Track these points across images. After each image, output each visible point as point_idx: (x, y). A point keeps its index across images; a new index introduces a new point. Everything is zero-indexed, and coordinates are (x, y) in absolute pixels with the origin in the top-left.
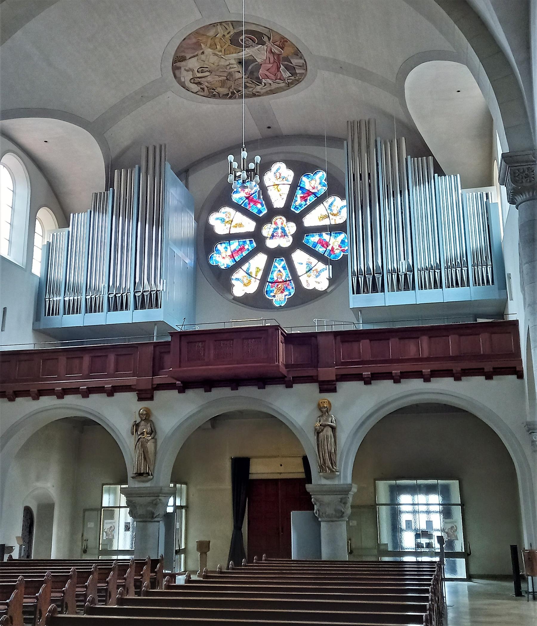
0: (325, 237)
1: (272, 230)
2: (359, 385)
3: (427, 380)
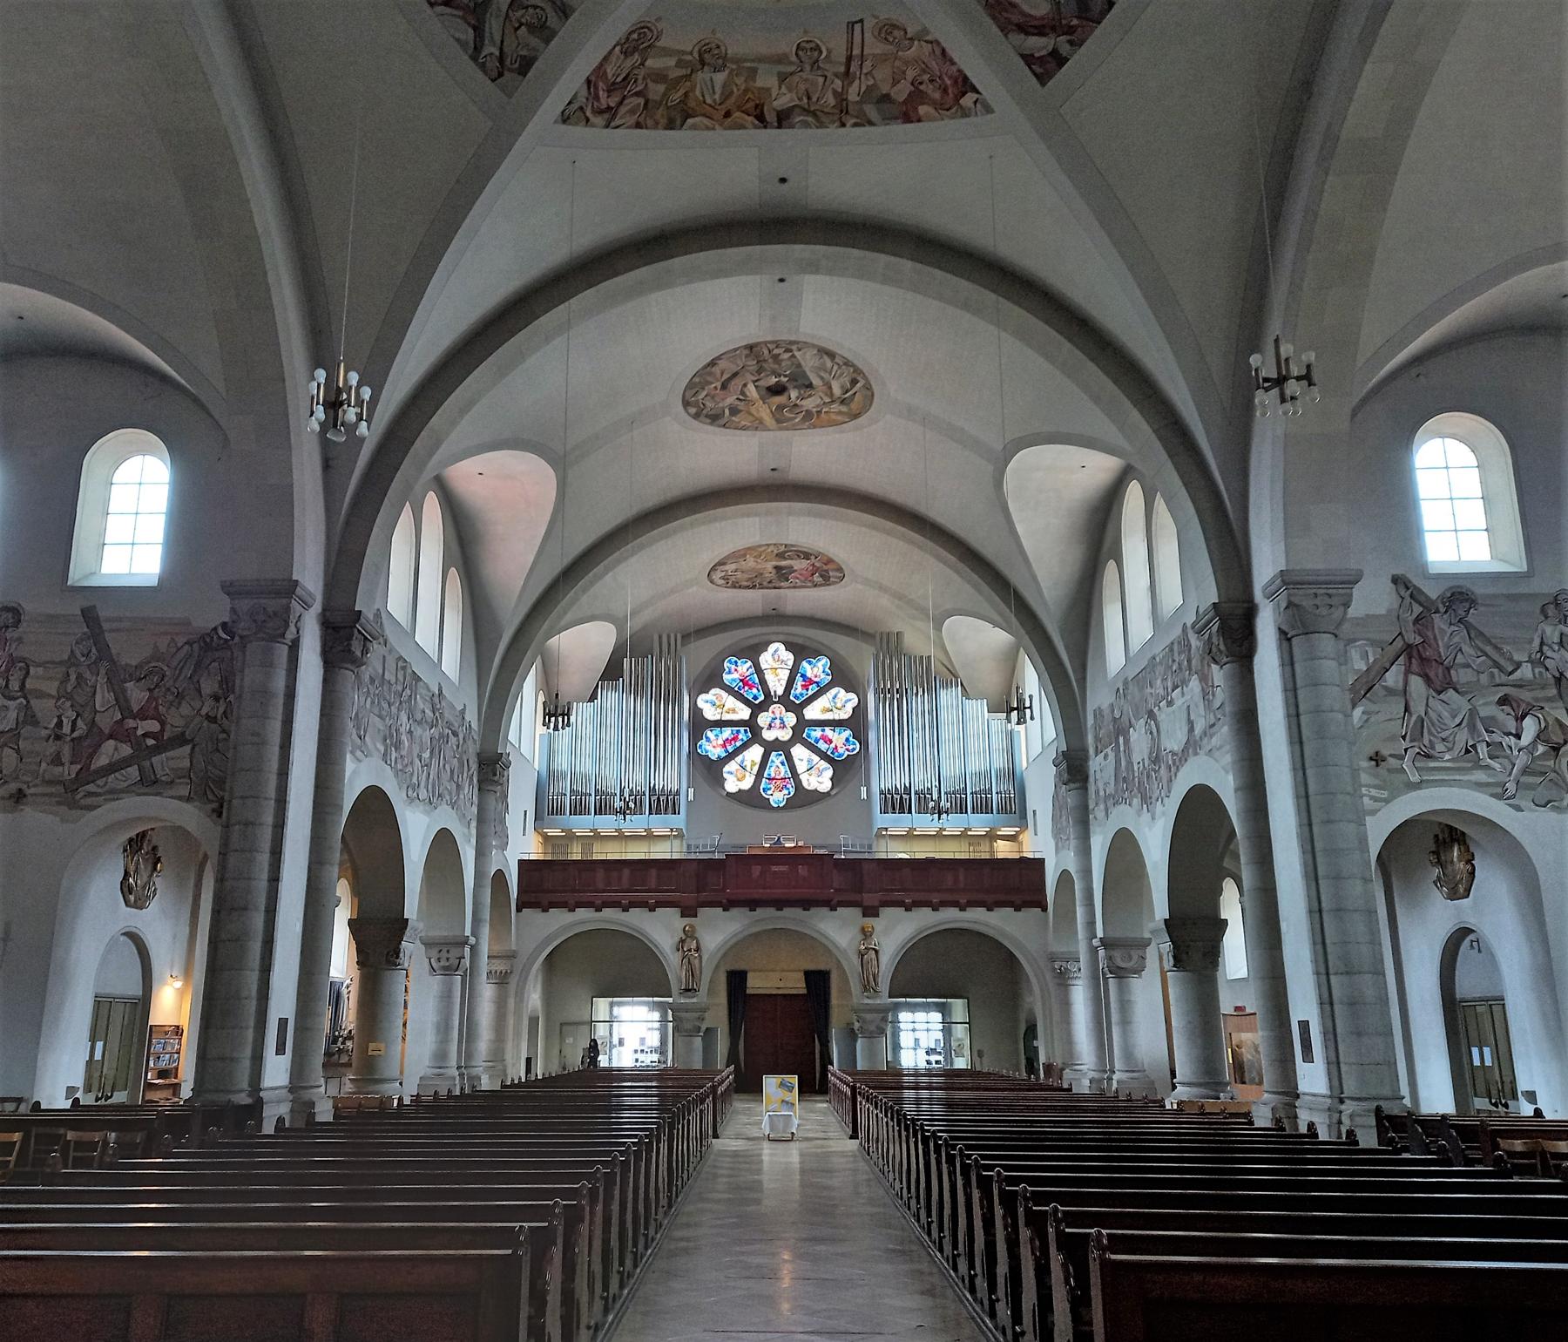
0: (828, 732)
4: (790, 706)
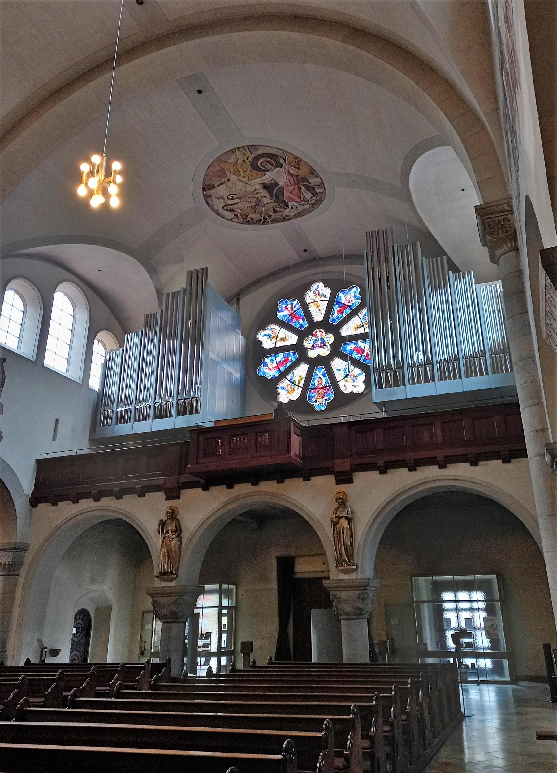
0: (361, 344)
1: (312, 341)
2: (374, 475)
3: (443, 466)
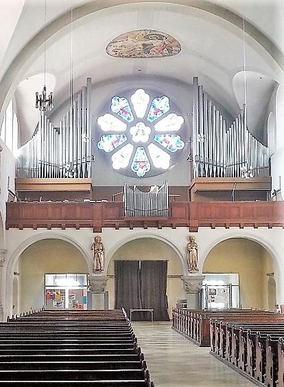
0: (168, 138)
4: (147, 124)
